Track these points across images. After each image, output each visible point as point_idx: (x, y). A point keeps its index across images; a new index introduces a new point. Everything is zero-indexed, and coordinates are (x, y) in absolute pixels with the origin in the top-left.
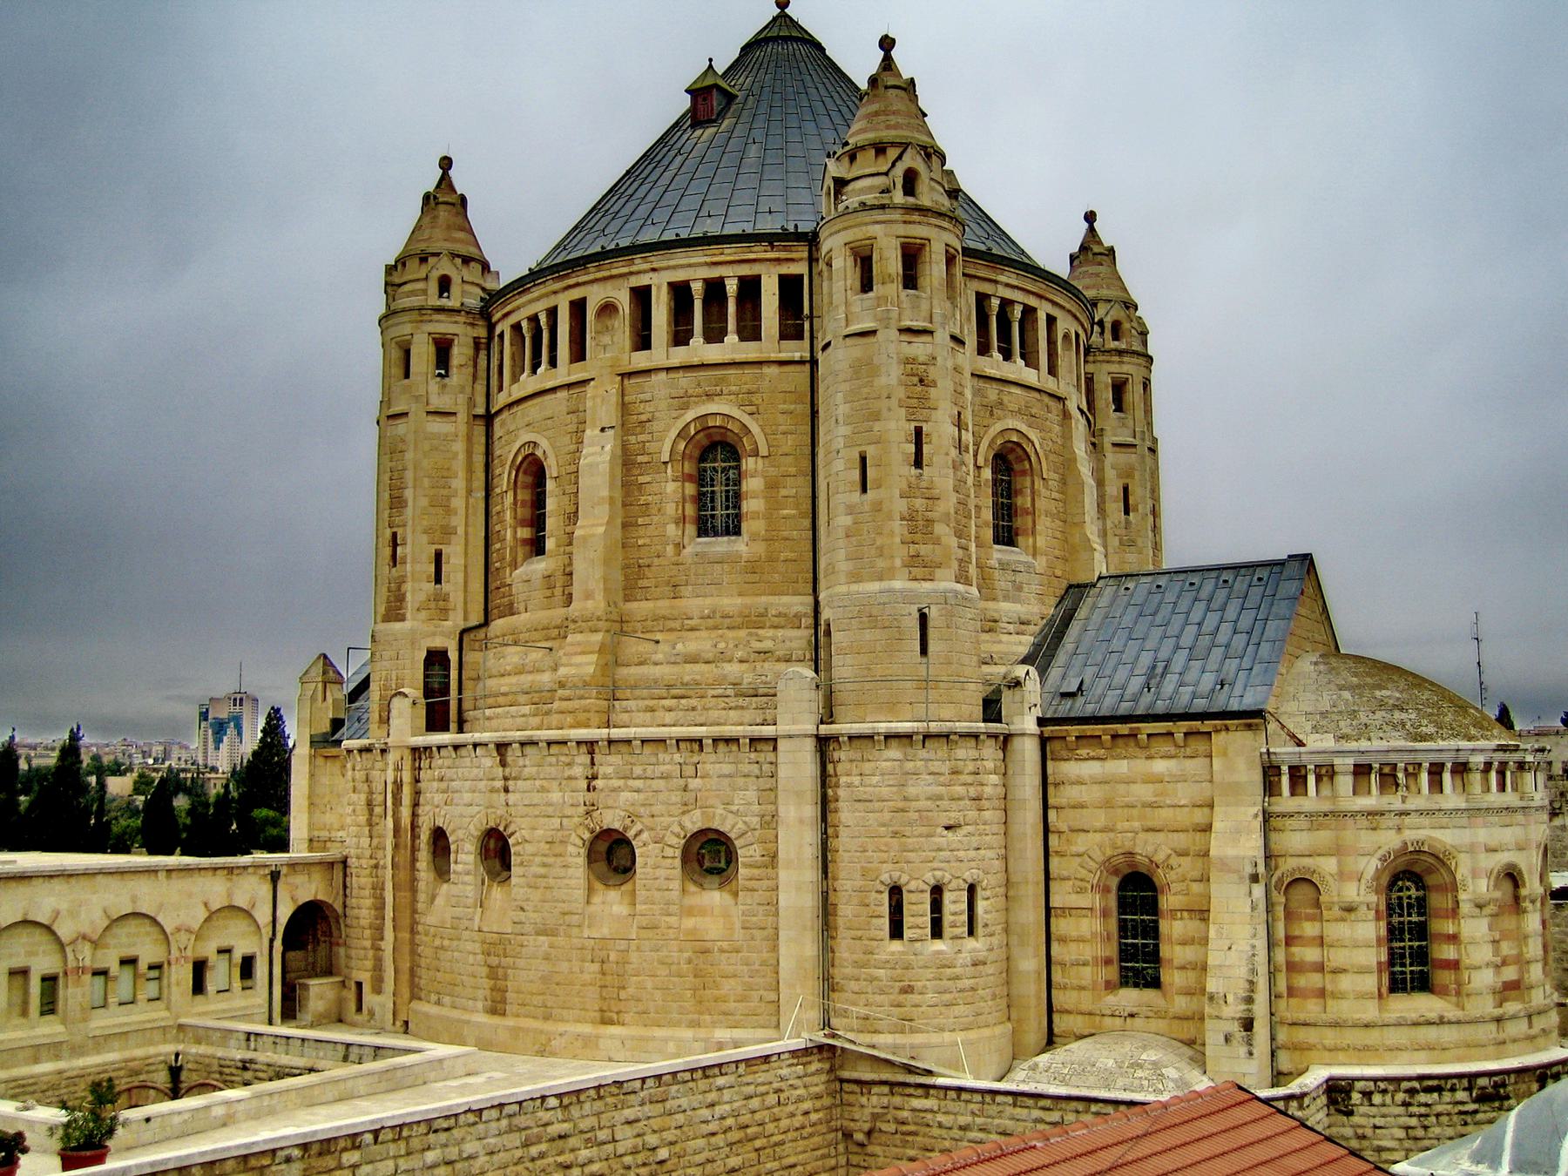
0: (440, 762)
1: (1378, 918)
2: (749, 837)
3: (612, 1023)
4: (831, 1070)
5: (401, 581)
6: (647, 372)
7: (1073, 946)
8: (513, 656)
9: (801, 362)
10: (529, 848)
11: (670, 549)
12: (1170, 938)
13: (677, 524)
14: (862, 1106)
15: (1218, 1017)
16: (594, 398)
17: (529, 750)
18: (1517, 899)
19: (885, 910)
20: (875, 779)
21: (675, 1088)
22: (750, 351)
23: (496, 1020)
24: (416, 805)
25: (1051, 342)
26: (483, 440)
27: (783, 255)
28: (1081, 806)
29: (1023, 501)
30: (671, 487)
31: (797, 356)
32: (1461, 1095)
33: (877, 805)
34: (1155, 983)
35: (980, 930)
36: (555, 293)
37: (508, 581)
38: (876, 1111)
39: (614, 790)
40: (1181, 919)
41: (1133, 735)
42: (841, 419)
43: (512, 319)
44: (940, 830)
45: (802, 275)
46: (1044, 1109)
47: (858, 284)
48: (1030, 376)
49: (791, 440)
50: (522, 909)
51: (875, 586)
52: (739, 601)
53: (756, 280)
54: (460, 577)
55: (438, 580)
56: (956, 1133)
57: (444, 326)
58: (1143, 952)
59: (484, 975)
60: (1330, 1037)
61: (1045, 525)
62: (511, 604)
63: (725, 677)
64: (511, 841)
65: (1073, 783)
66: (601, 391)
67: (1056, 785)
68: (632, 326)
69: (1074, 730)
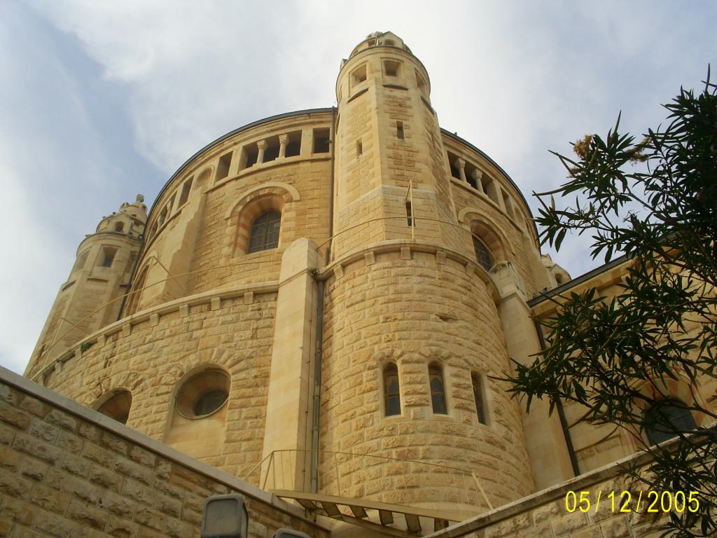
6: (223, 184)
44: (433, 316)
45: (328, 130)
49: (316, 192)
53: (299, 134)
68: (217, 172)
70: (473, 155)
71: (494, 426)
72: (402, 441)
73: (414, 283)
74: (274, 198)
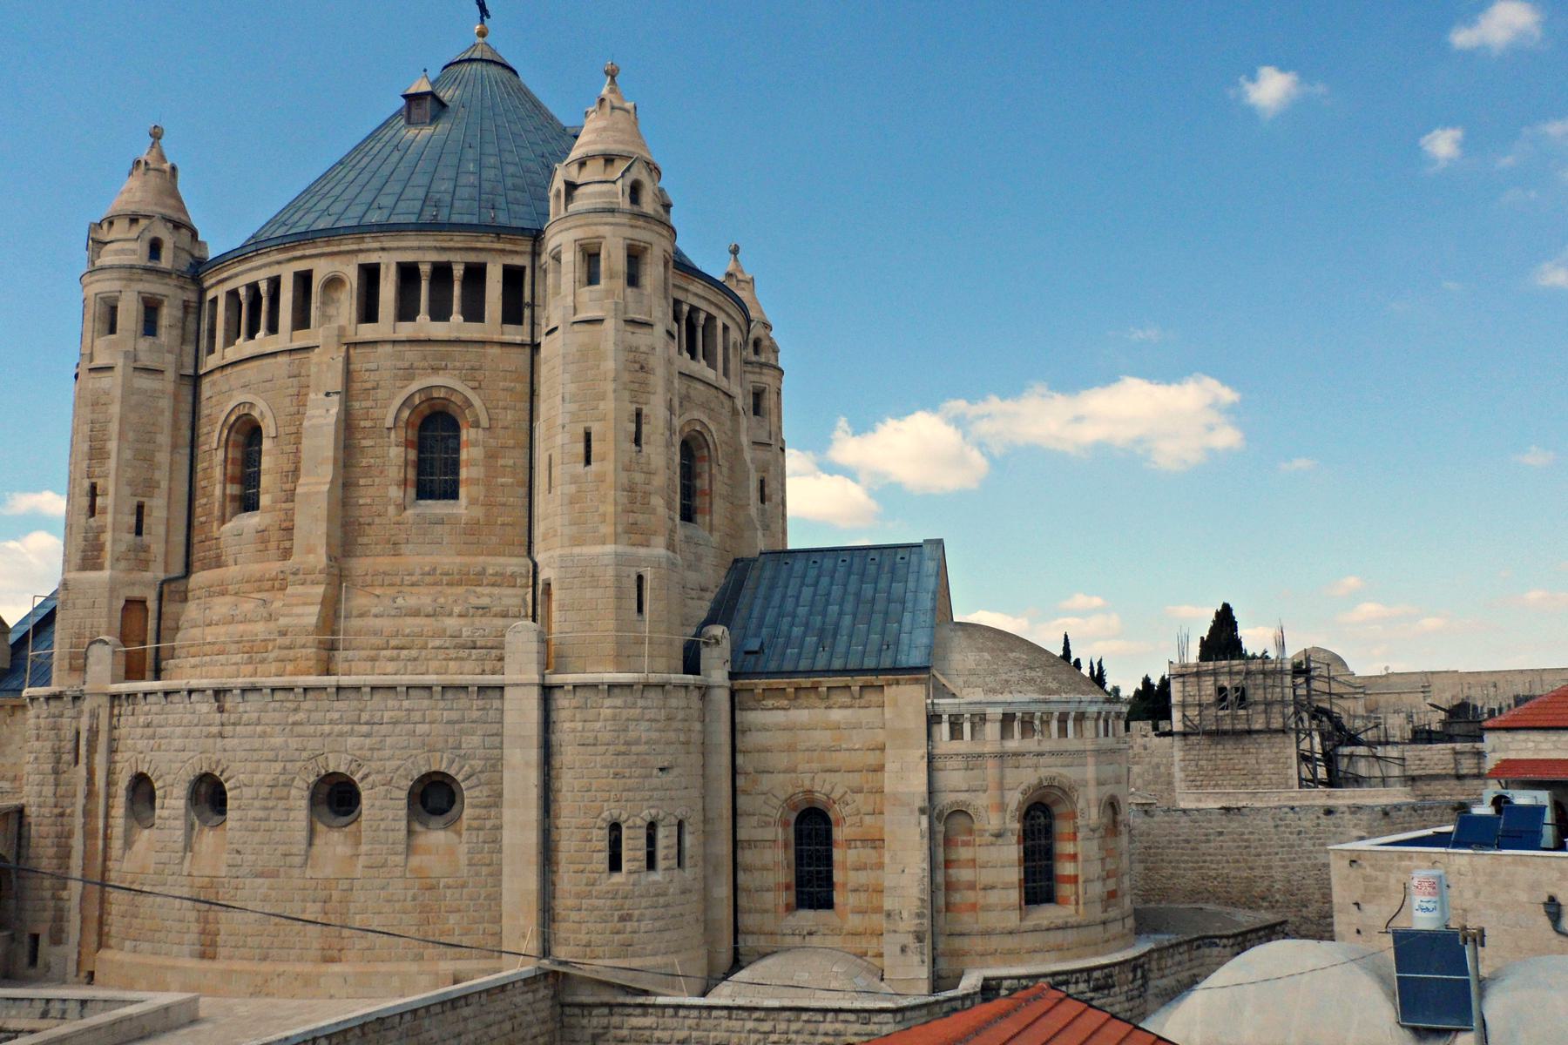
0: (147, 708)
1: (1019, 843)
2: (474, 780)
3: (332, 960)
4: (554, 997)
5: (101, 530)
7: (757, 874)
8: (221, 607)
9: (522, 345)
10: (248, 792)
11: (391, 510)
12: (844, 863)
13: (399, 486)
14: (583, 1027)
15: (895, 932)
16: (319, 364)
17: (251, 696)
18: (1115, 823)
19: (605, 844)
20: (598, 725)
21: (427, 1022)
22: (473, 331)
23: (206, 964)
24: (112, 751)
25: (726, 349)
26: (190, 399)
27: (508, 247)
29: (702, 483)
31: (518, 339)
32: (1082, 986)
33: (602, 749)
34: (828, 904)
35: (687, 862)
36: (279, 263)
37: (216, 535)
38: (597, 1031)
39: (341, 735)
40: (856, 848)
42: (567, 397)
43: (229, 286)
44: (655, 771)
45: (523, 269)
46: (756, 1020)
47: (585, 279)
48: (710, 374)
49: (510, 415)
50: (238, 852)
51: (598, 549)
52: (458, 560)
54: (161, 530)
55: (139, 532)
57: (154, 287)
58: (818, 879)
59: (193, 919)
60: (978, 944)
61: (719, 506)
62: (218, 557)
63: (444, 630)
64: (227, 786)
65: (759, 730)
66: (326, 358)
67: (744, 732)
69: (762, 683)
72: (622, 905)
73: (641, 731)
74: (452, 405)
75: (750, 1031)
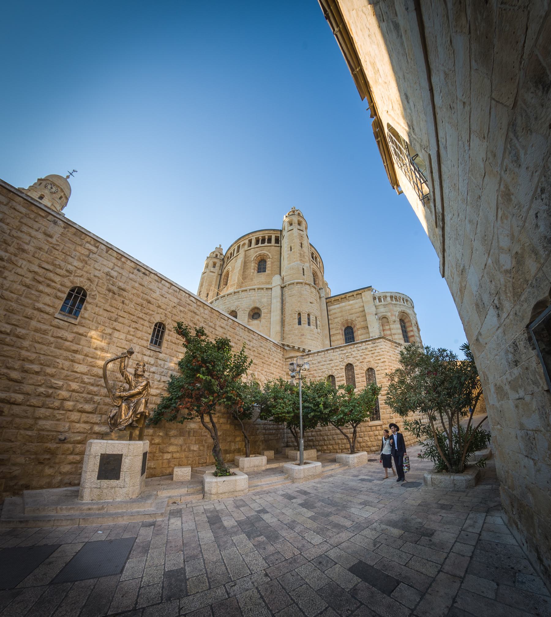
2: (264, 308)
6: (250, 249)
28: (336, 313)
30: (253, 264)
41: (345, 298)
46: (342, 350)
56: (317, 365)
67: (330, 311)
70: (314, 250)
71: (319, 330)
75: (340, 354)
